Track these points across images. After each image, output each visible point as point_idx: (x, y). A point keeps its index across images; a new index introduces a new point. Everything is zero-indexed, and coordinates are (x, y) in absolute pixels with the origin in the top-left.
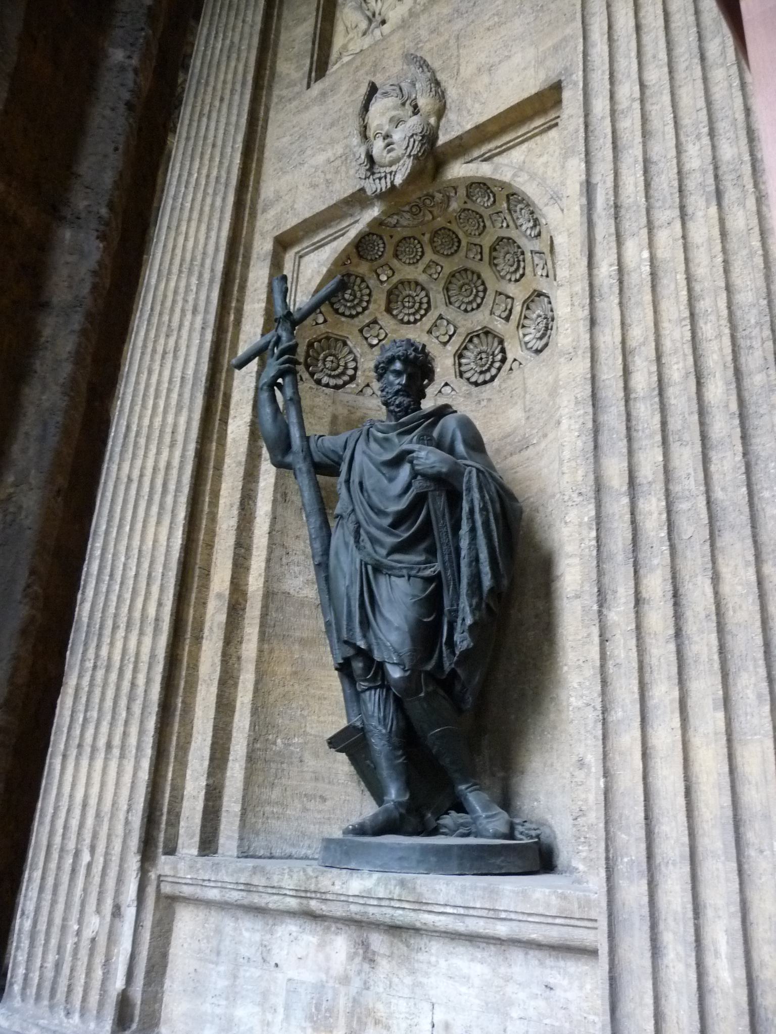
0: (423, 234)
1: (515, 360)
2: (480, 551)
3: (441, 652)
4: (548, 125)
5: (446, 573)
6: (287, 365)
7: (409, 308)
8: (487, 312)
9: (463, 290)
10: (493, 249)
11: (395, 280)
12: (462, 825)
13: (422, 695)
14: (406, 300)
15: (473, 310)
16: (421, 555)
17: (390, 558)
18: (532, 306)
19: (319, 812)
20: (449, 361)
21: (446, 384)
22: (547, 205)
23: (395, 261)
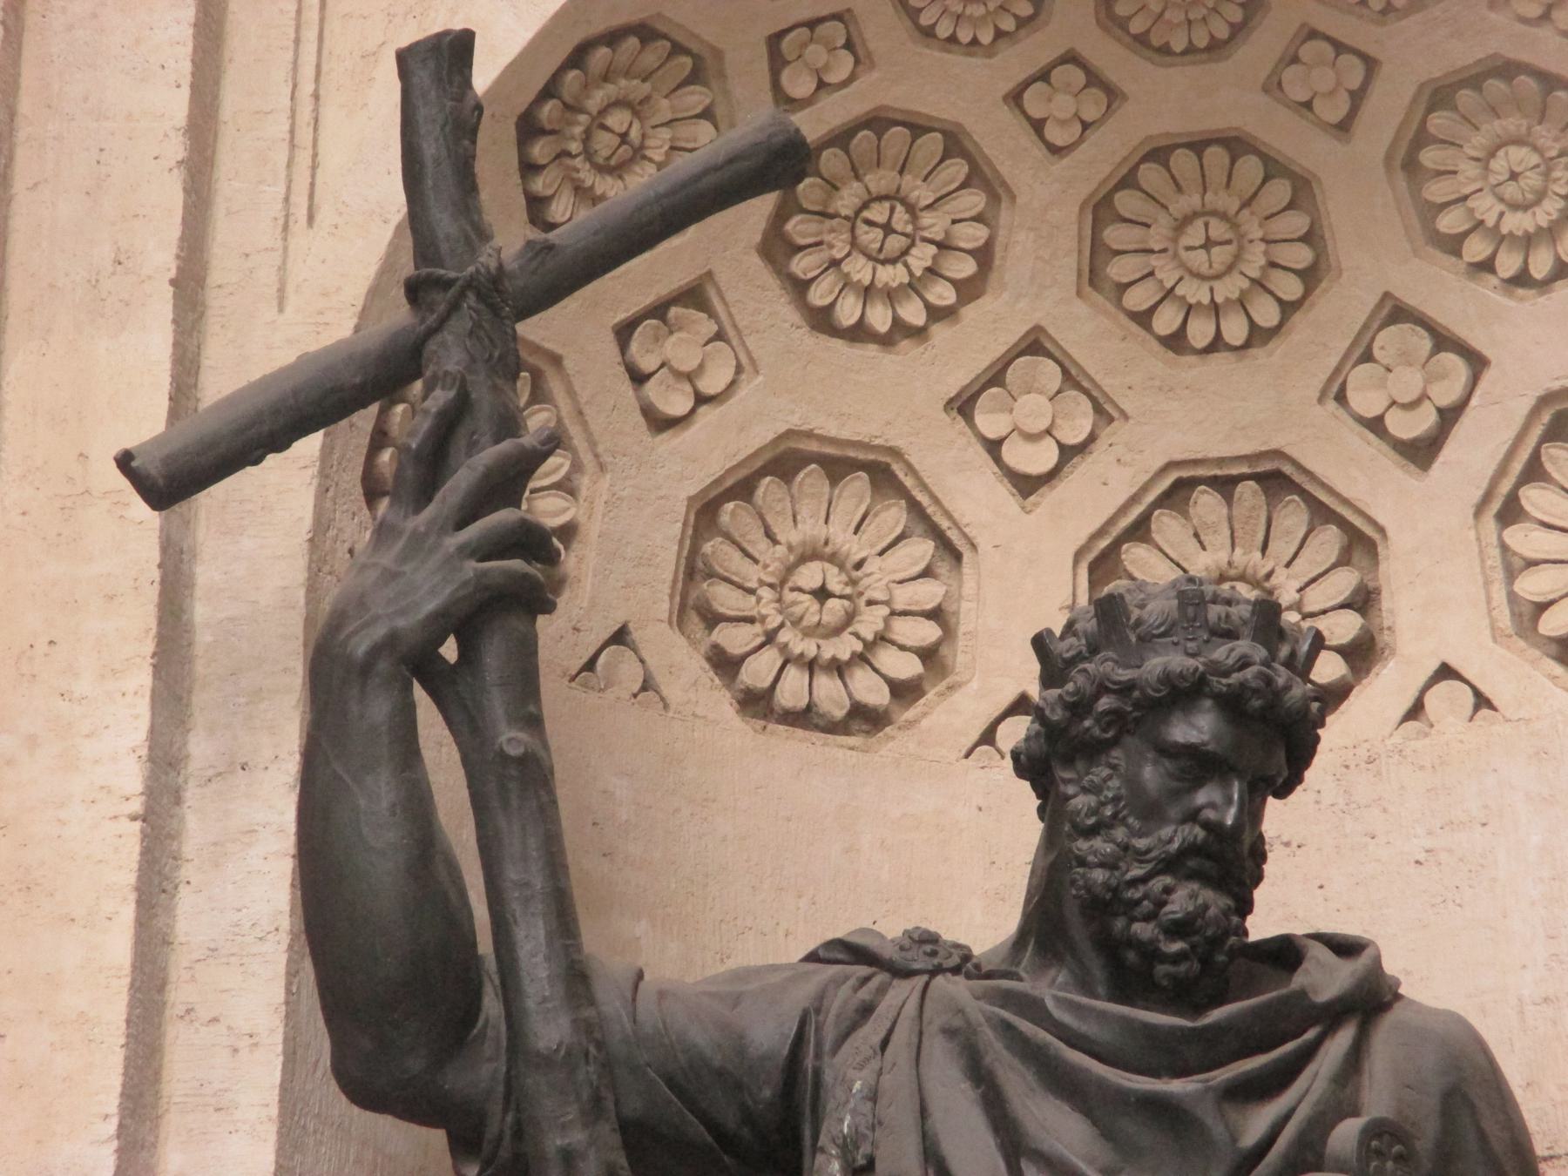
1: (1446, 672)
6: (516, 564)
7: (879, 259)
9: (1194, 234)
10: (1439, 95)
14: (878, 213)
15: (1217, 344)
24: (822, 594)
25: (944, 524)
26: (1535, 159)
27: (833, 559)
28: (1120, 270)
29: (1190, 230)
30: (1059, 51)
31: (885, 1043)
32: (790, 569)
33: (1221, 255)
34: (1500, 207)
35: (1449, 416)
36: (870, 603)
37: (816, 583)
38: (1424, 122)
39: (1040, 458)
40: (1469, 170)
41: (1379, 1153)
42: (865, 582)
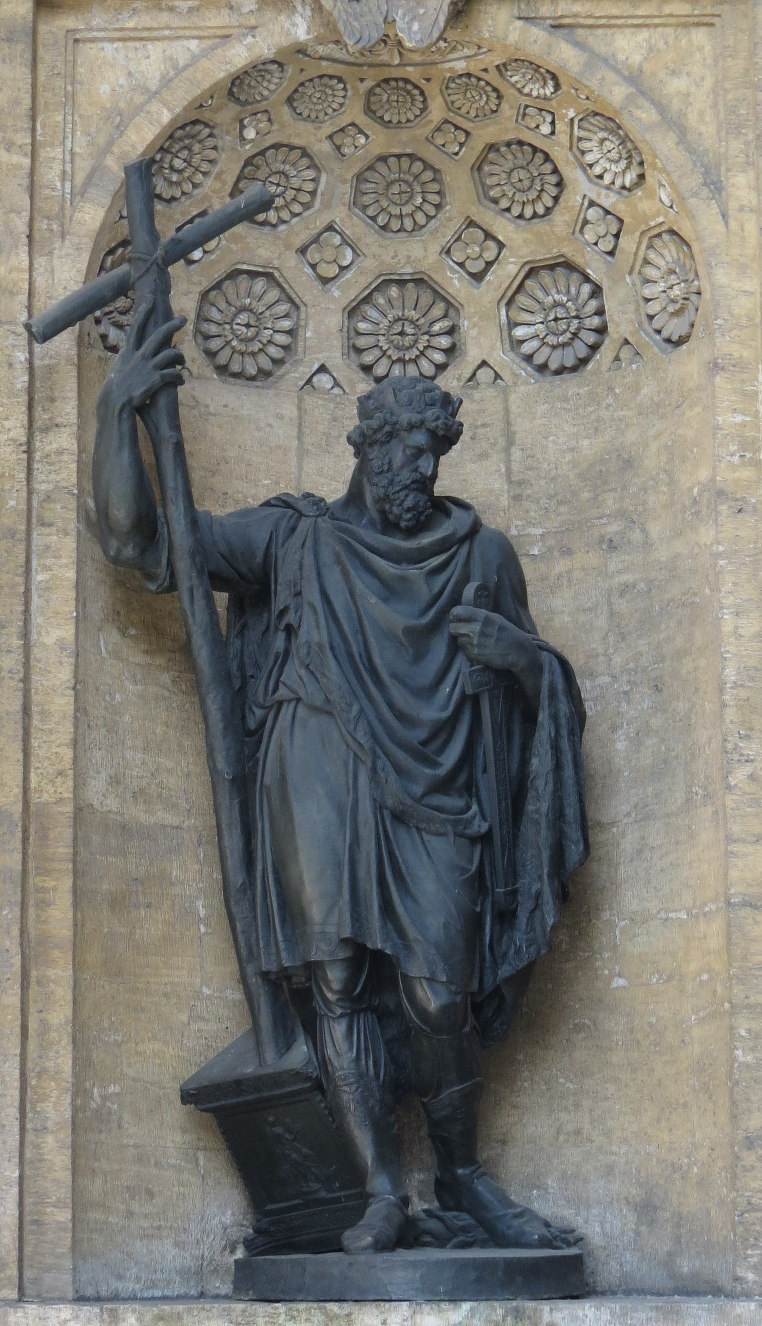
0: (362, 80)
2: (566, 802)
3: (483, 959)
4: (696, 20)
5: (501, 829)
8: (434, 248)
9: (395, 189)
11: (269, 141)
12: (465, 1230)
16: (461, 796)
17: (428, 800)
18: (546, 277)
19: (146, 1216)
20: (335, 320)
21: (322, 369)
22: (696, 194)
23: (286, 110)
24: (248, 326)
25: (294, 296)
26: (528, 175)
27: (251, 311)
28: (366, 199)
29: (394, 187)
30: (350, 122)
31: (303, 545)
32: (235, 316)
33: (405, 197)
34: (514, 190)
35: (489, 264)
36: (265, 328)
37: (245, 322)
38: (486, 155)
39: (333, 271)
40: (504, 176)
41: (480, 596)
42: (262, 321)
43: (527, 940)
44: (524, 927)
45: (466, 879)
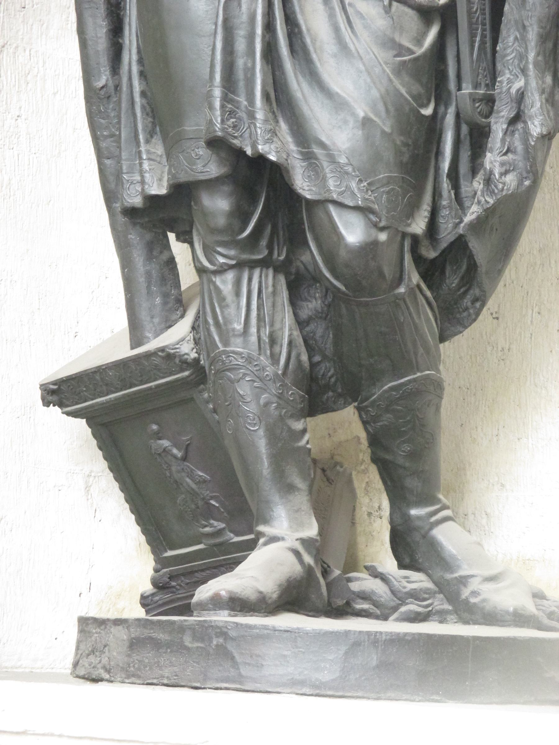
3: (437, 194)
12: (415, 595)
13: (402, 290)
43: (502, 164)
44: (498, 145)
45: (404, 62)
